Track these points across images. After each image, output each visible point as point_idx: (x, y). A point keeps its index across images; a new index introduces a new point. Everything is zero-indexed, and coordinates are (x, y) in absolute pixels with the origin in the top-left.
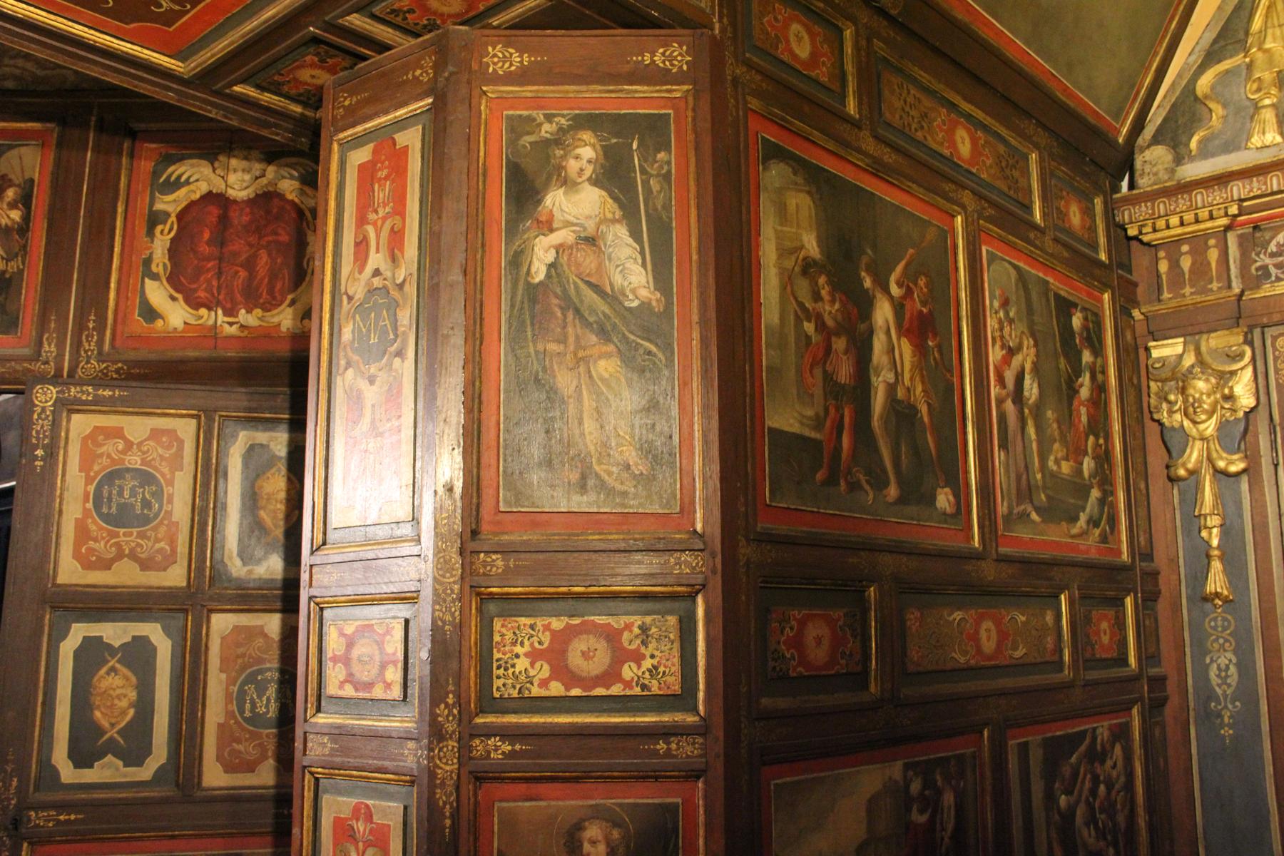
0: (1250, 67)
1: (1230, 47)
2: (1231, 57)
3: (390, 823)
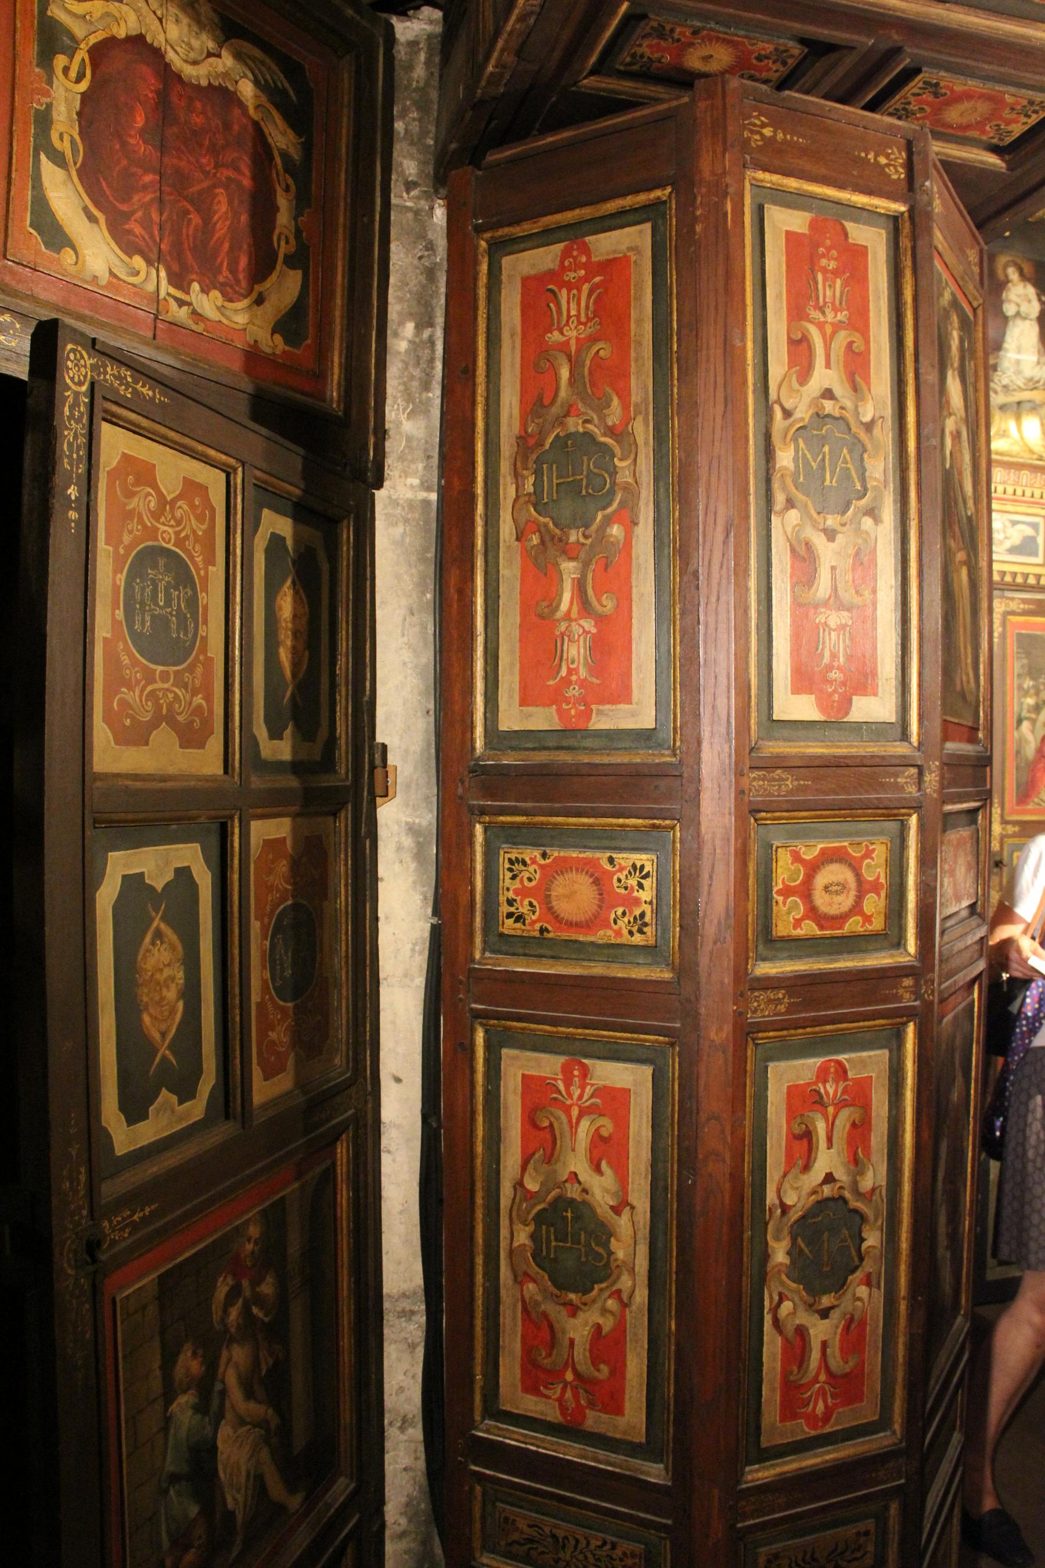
3: (873, 1075)
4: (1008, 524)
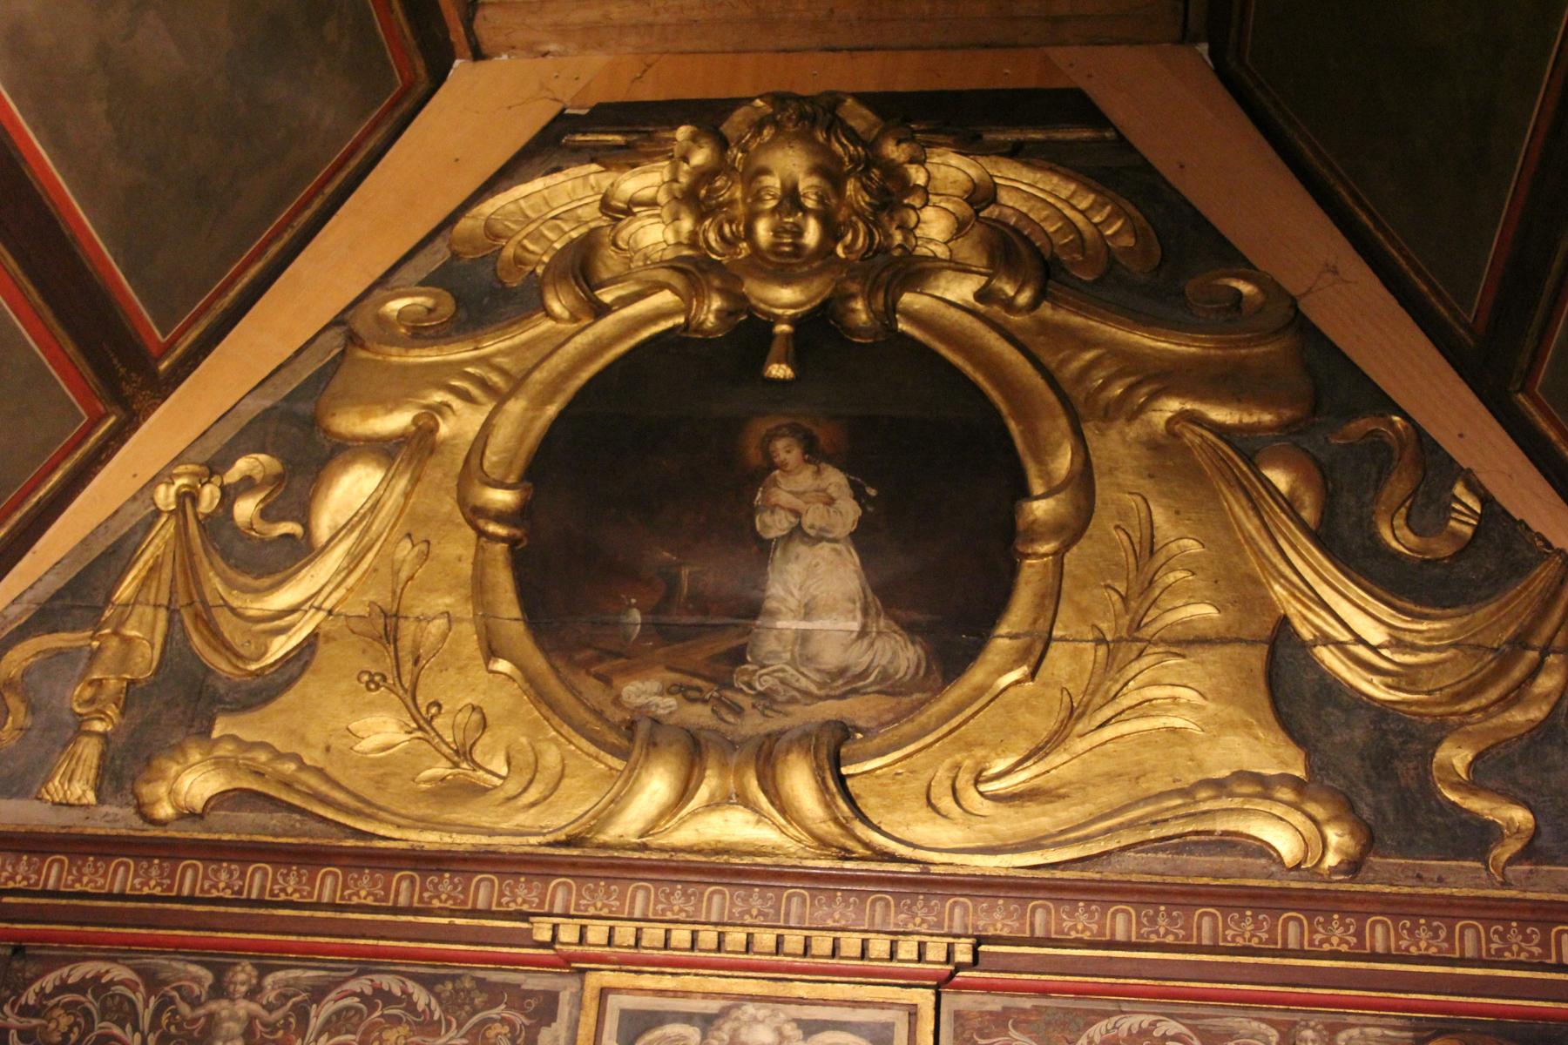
0: (94, 655)
1: (77, 613)
2: (74, 630)
4: (790, 1029)
